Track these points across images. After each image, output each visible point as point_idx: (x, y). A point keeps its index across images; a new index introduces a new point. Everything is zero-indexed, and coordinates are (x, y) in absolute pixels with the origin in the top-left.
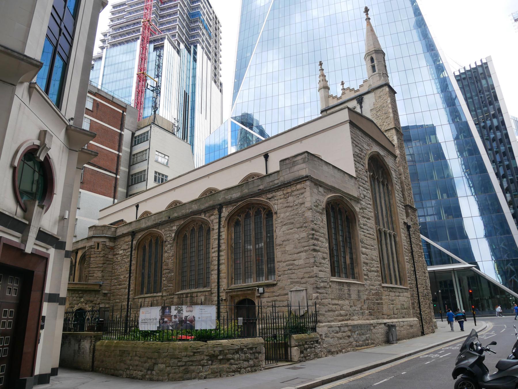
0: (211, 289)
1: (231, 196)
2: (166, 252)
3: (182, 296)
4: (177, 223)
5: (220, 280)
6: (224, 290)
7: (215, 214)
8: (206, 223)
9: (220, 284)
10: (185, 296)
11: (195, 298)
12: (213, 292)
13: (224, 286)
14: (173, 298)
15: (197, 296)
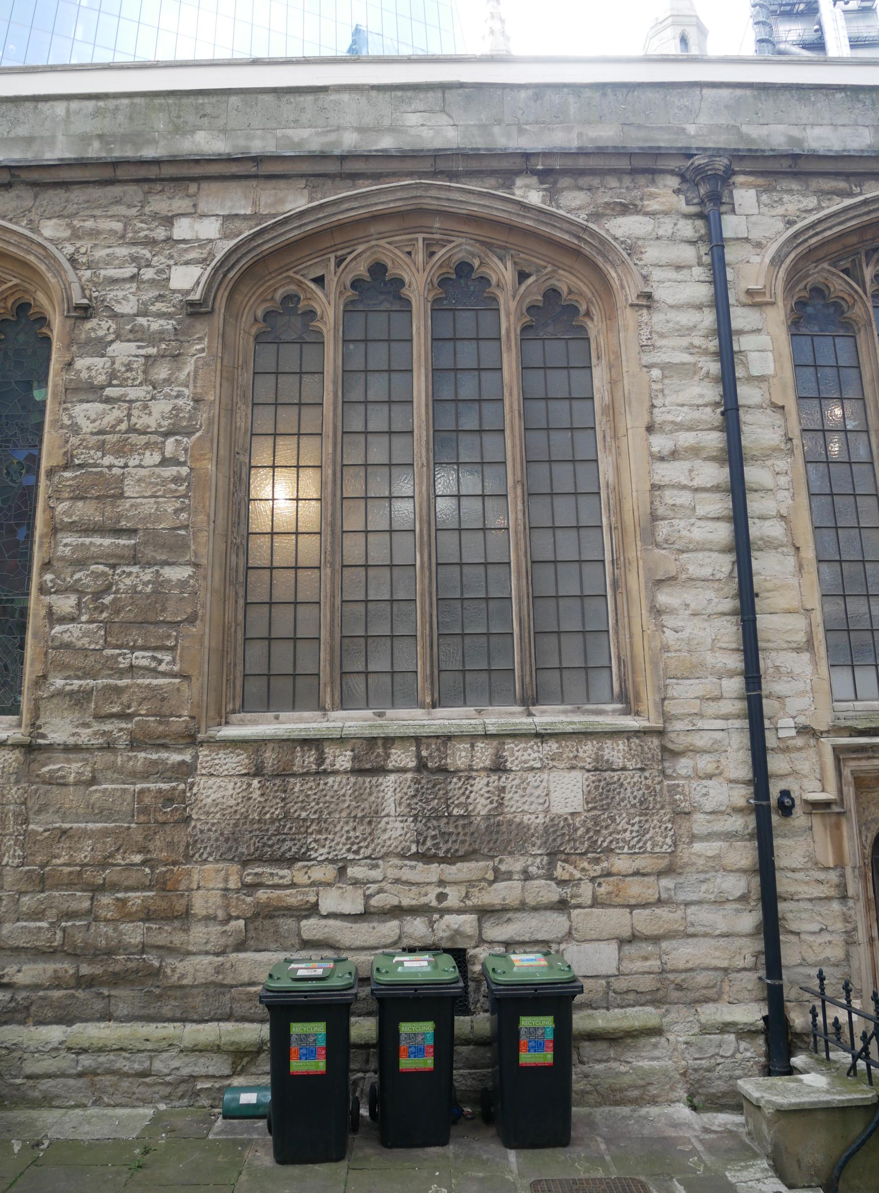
0: (666, 717)
1: (795, 132)
2: (91, 391)
3: (306, 760)
4: (237, 201)
5: (766, 663)
6: (804, 730)
7: (653, 205)
8: (582, 252)
9: (768, 686)
10: (343, 760)
11: (480, 783)
12: (679, 742)
13: (795, 704)
14: (186, 770)
15: (498, 768)
